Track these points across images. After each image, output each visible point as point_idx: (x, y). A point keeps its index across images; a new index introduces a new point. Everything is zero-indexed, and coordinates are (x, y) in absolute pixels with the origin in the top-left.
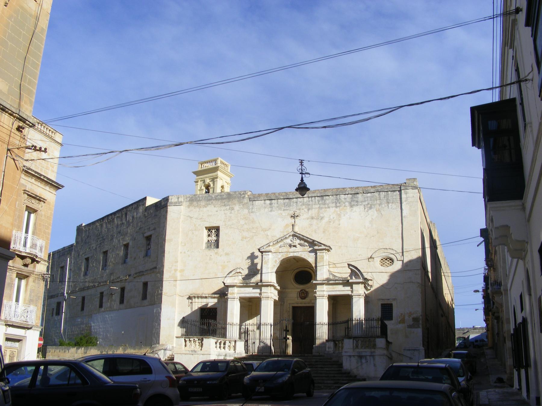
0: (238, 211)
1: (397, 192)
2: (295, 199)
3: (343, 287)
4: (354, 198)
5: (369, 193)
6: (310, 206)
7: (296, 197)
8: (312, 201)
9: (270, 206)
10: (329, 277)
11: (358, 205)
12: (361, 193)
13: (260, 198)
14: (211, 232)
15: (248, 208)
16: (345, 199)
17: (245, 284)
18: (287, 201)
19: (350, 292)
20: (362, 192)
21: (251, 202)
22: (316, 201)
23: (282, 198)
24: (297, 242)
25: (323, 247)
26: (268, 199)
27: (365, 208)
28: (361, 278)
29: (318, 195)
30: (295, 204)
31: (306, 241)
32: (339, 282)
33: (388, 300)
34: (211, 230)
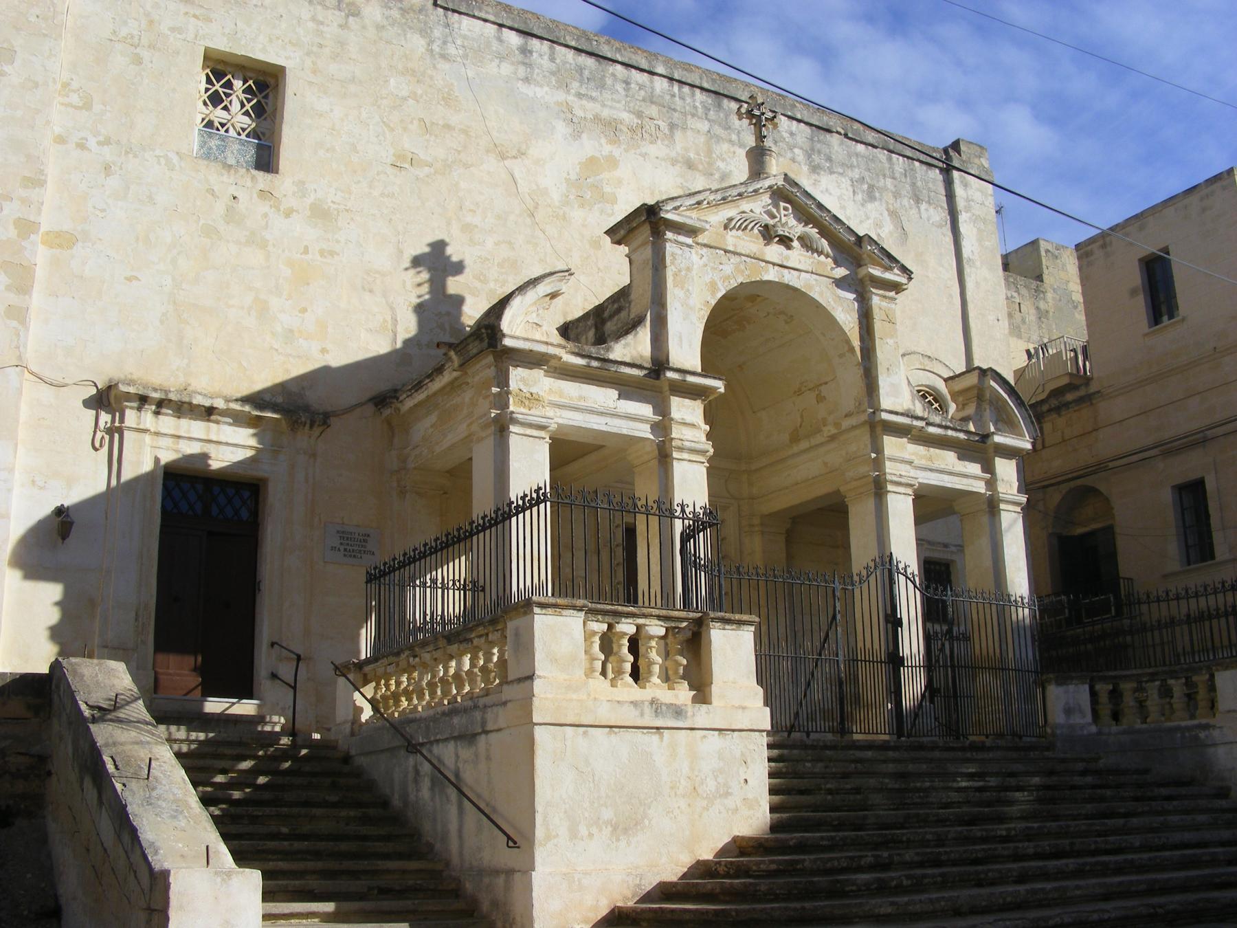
0: (380, 28)
1: (937, 171)
2: (619, 67)
3: (959, 459)
4: (819, 141)
5: (862, 142)
6: (676, 115)
7: (626, 60)
8: (682, 98)
9: (520, 57)
10: (912, 407)
11: (834, 173)
12: (838, 132)
13: (480, 10)
14: (229, 85)
15: (425, 32)
16: (792, 134)
17: (595, 364)
18: (590, 62)
19: (982, 484)
20: (843, 132)
21: (440, 11)
22: (698, 104)
23: (573, 44)
24: (792, 226)
25: (894, 276)
26: (516, 26)
27: (854, 191)
28: (1022, 435)
29: (706, 85)
30: (620, 87)
31: (824, 232)
32: (957, 438)
33: (946, 546)
34: (229, 76)
